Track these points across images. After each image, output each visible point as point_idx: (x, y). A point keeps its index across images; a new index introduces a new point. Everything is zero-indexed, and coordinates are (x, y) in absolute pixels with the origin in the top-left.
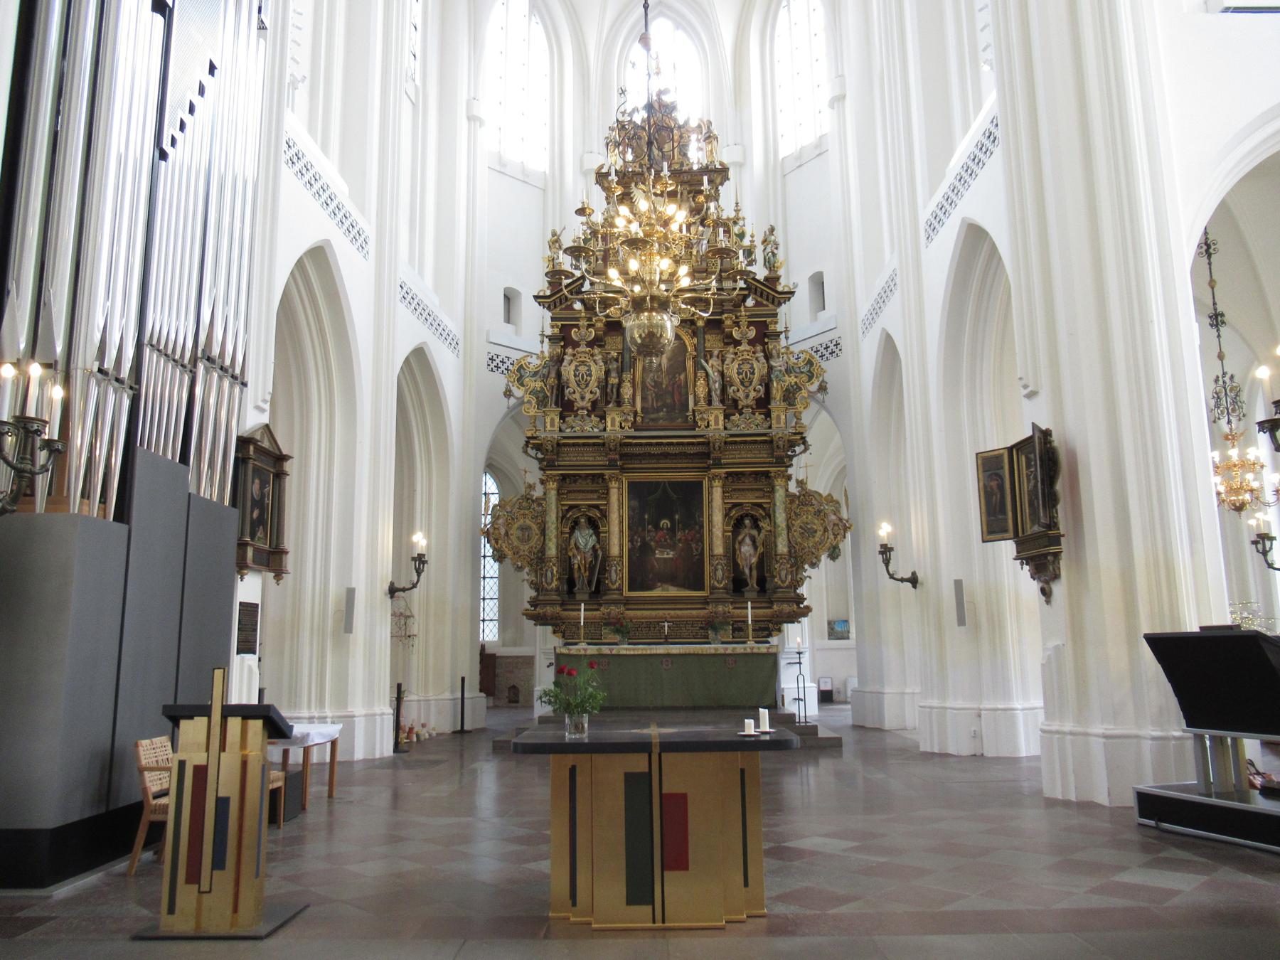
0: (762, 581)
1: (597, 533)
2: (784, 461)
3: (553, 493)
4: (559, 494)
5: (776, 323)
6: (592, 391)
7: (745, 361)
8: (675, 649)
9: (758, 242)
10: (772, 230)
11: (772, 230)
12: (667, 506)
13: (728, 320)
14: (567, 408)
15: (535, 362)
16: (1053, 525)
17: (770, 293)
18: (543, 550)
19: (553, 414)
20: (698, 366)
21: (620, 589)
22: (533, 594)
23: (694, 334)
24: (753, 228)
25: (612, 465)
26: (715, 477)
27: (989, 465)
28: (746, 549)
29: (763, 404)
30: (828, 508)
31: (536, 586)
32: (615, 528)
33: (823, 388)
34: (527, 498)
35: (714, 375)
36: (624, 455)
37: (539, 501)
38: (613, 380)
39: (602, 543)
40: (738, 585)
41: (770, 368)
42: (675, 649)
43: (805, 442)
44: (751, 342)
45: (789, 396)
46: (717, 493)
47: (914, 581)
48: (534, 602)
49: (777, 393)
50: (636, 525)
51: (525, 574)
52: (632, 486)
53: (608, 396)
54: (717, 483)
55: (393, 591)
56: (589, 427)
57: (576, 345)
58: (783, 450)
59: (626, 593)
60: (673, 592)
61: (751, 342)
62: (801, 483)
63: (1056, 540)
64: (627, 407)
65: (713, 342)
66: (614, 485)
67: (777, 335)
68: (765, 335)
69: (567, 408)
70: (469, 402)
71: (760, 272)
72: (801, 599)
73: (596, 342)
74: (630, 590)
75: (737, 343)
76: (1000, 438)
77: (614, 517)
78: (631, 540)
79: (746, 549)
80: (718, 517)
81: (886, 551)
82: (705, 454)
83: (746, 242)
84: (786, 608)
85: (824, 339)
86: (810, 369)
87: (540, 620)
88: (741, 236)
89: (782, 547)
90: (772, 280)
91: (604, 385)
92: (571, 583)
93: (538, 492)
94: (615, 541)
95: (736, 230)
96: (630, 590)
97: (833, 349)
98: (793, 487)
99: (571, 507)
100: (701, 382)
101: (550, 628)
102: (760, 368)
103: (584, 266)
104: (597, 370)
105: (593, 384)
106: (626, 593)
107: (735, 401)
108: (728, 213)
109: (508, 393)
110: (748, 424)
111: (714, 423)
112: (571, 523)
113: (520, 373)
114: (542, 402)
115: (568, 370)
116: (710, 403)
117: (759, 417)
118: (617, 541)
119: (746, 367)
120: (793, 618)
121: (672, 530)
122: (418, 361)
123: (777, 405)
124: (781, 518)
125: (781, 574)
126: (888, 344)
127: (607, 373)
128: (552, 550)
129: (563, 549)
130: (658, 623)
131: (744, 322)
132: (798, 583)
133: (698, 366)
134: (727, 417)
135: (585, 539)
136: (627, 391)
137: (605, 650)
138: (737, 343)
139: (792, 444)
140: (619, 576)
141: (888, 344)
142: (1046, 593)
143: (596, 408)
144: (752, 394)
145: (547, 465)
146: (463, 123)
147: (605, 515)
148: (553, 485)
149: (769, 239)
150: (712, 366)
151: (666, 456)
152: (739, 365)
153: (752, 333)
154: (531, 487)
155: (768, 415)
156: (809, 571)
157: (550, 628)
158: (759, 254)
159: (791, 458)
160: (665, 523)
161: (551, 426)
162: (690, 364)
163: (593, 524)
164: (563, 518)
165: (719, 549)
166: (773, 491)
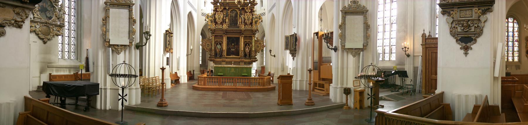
0: (249, 55)
2: (254, 34)
6: (221, 20)
8: (234, 66)
12: (233, 41)
13: (245, 8)
14: (216, 23)
15: (210, 14)
16: (295, 48)
19: (214, 24)
20: (240, 16)
25: (224, 34)
27: (287, 38)
28: (247, 49)
29: (251, 24)
31: (210, 55)
33: (262, 21)
35: (243, 18)
36: (226, 32)
39: (222, 47)
40: (245, 55)
45: (256, 22)
46: (242, 39)
47: (274, 56)
48: (210, 58)
49: (254, 22)
50: (228, 44)
52: (228, 38)
53: (224, 21)
56: (220, 27)
58: (254, 32)
60: (234, 56)
63: (296, 51)
65: (243, 12)
68: (252, 11)
69: (216, 23)
70: (199, 22)
76: (288, 34)
77: (224, 43)
79: (247, 49)
80: (242, 44)
81: (270, 51)
82: (241, 32)
86: (260, 17)
87: (211, 60)
89: (253, 49)
91: (223, 19)
92: (216, 54)
98: (256, 39)
102: (251, 17)
104: (222, 16)
109: (205, 20)
110: (248, 27)
111: (243, 27)
112: (216, 43)
113: (208, 16)
114: (212, 22)
115: (217, 16)
118: (225, 47)
120: (255, 61)
121: (234, 46)
123: (254, 23)
124: (253, 44)
125: (253, 54)
126: (273, 16)
128: (213, 49)
129: (215, 48)
130: (231, 62)
132: (256, 55)
133: (240, 16)
136: (227, 20)
139: (256, 31)
140: (225, 53)
141: (273, 16)
142: (293, 59)
143: (222, 23)
145: (213, 33)
151: (233, 32)
152: (247, 16)
153: (250, 11)
161: (213, 26)
163: (220, 44)
164: (215, 43)
165: (242, 49)
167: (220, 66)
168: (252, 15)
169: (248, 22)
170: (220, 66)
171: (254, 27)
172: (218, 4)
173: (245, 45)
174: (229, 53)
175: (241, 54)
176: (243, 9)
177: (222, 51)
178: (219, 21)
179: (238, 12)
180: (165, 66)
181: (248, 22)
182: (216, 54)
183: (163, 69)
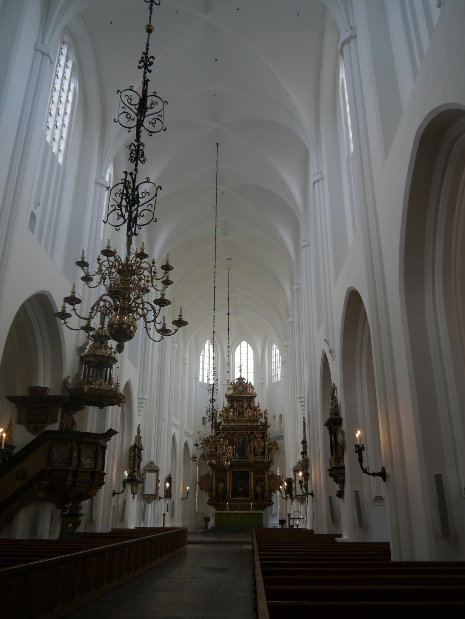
1: (224, 483)
3: (214, 475)
4: (216, 474)
8: (241, 512)
9: (263, 412)
10: (266, 410)
11: (266, 410)
17: (266, 426)
18: (212, 487)
20: (248, 444)
21: (229, 498)
22: (209, 498)
23: (248, 435)
24: (263, 408)
26: (252, 471)
28: (259, 488)
29: (263, 453)
30: (278, 478)
32: (228, 483)
33: (278, 449)
34: (208, 475)
35: (252, 446)
37: (211, 476)
39: (226, 486)
40: (257, 496)
41: (265, 445)
42: (241, 512)
43: (273, 462)
44: (260, 438)
46: (252, 475)
48: (209, 500)
49: (266, 451)
50: (233, 482)
51: (207, 493)
54: (252, 472)
55: (182, 499)
60: (242, 498)
61: (260, 438)
62: (272, 472)
66: (228, 473)
67: (267, 436)
68: (264, 435)
71: (263, 420)
72: (272, 501)
74: (232, 497)
75: (257, 438)
77: (228, 480)
79: (259, 488)
80: (252, 481)
82: (249, 465)
83: (260, 412)
84: (267, 503)
85: (280, 434)
87: (211, 505)
88: (259, 411)
90: (266, 422)
93: (211, 473)
94: (228, 486)
95: (258, 409)
96: (232, 497)
97: (282, 437)
99: (218, 477)
100: (249, 448)
101: (213, 507)
103: (222, 418)
107: (257, 453)
108: (256, 405)
110: (259, 459)
111: (252, 459)
116: (251, 453)
117: (262, 456)
119: (259, 444)
122: (186, 445)
123: (266, 453)
124: (267, 481)
128: (214, 488)
129: (217, 487)
131: (259, 433)
132: (271, 496)
134: (255, 456)
135: (221, 485)
137: (225, 512)
138: (257, 438)
139: (270, 463)
140: (229, 494)
144: (261, 451)
146: (194, 380)
147: (226, 479)
148: (214, 472)
149: (266, 412)
152: (257, 443)
153: (261, 436)
154: (209, 472)
155: (264, 456)
156: (274, 494)
157: (213, 507)
158: (263, 415)
159: (269, 466)
160: (240, 481)
162: (246, 441)
165: (252, 489)
166: (265, 474)
167: (222, 512)
168: (264, 441)
170: (222, 512)
171: (266, 460)
172: (221, 427)
173: (258, 481)
174: (235, 494)
175: (251, 494)
176: (252, 433)
177: (225, 491)
180: (166, 513)
181: (259, 451)
182: (218, 495)
183: (164, 515)
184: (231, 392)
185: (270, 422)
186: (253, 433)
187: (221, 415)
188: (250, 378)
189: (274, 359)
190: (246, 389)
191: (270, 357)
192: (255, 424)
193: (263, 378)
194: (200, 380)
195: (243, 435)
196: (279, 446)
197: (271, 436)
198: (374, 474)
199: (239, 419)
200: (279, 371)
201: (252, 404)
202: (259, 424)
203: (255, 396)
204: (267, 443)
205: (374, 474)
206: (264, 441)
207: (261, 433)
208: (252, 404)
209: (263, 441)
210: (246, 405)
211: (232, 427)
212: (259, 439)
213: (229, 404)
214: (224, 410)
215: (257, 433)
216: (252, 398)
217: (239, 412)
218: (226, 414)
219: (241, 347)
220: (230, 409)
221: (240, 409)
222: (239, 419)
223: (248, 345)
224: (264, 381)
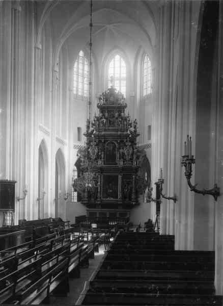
5: (136, 141)
7: (128, 150)
9: (133, 122)
13: (125, 140)
14: (89, 158)
17: (135, 135)
24: (132, 119)
38: (100, 154)
41: (133, 152)
52: (104, 176)
57: (92, 146)
59: (102, 199)
61: (130, 146)
64: (103, 160)
68: (133, 142)
71: (132, 129)
73: (97, 145)
75: (126, 146)
78: (103, 187)
88: (129, 121)
90: (135, 131)
95: (128, 119)
96: (104, 198)
105: (96, 154)
106: (102, 199)
108: (127, 115)
110: (128, 164)
127: (98, 152)
134: (123, 162)
136: (102, 156)
150: (121, 150)
153: (130, 144)
156: (140, 196)
168: (133, 149)
169: (128, 158)
172: (93, 136)
176: (122, 141)
178: (93, 157)
179: (117, 145)
181: (128, 158)
184: (102, 103)
185: (138, 131)
186: (123, 141)
187: (93, 125)
188: (122, 89)
189: (145, 73)
190: (117, 100)
191: (142, 72)
192: (125, 133)
193: (135, 91)
194: (75, 92)
195: (113, 143)
196: (147, 153)
197: (140, 145)
198: (169, 198)
199: (110, 128)
200: (149, 84)
201: (122, 114)
202: (129, 132)
203: (126, 107)
204: (135, 150)
205: (169, 198)
206: (133, 149)
207: (130, 141)
208: (122, 114)
209: (131, 149)
210: (116, 114)
211: (104, 136)
212: (128, 147)
213: (101, 115)
214: (96, 119)
215: (127, 141)
216: (121, 108)
217: (110, 121)
218: (98, 123)
219: (114, 61)
220: (101, 118)
221: (111, 119)
222: (110, 128)
223: (122, 59)
224: (136, 94)
